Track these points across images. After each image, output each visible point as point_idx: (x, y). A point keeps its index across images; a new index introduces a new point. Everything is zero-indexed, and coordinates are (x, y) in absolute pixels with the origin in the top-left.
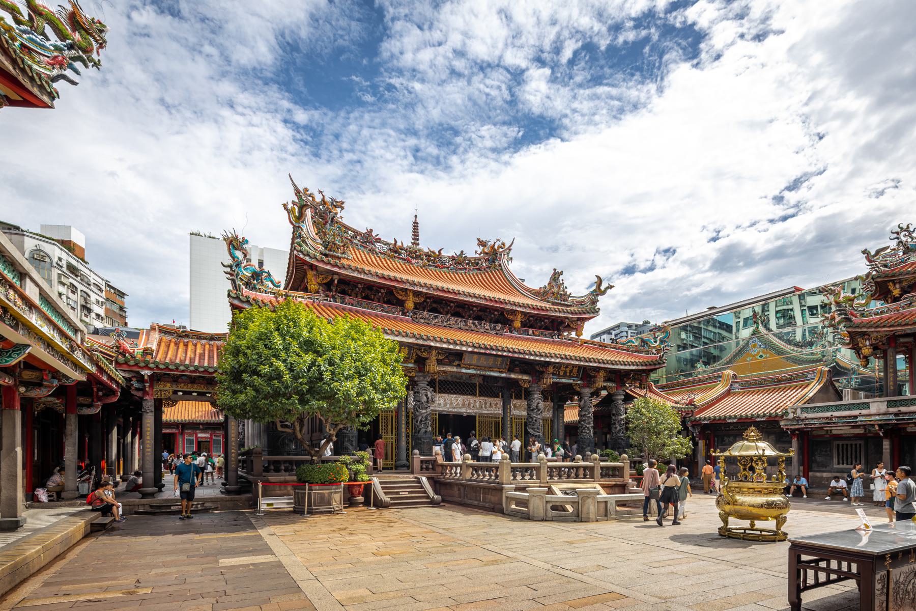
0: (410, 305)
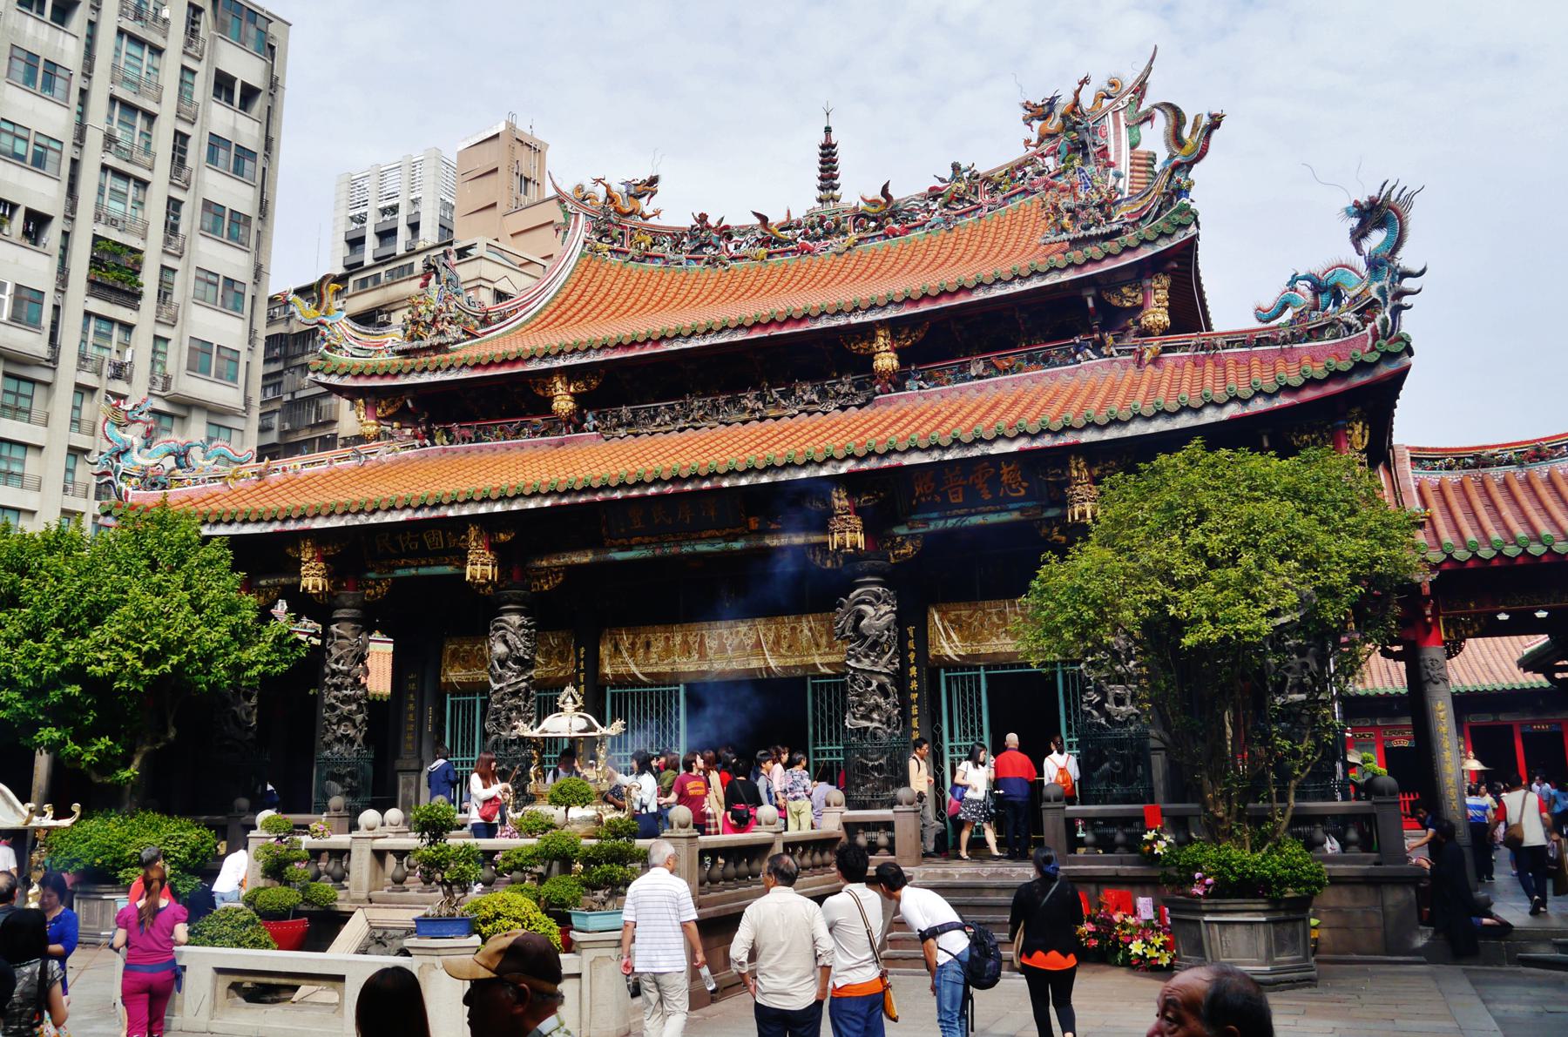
0: (563, 403)
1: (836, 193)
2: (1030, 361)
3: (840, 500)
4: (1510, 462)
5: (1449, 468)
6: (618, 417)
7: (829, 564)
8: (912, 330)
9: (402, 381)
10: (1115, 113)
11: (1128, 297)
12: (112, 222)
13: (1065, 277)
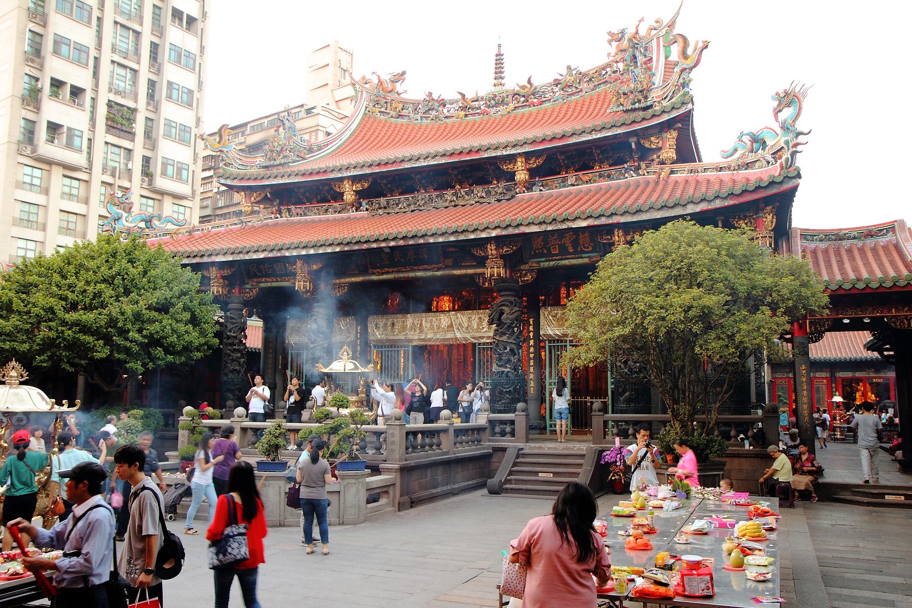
0: (349, 197)
1: (503, 81)
2: (600, 176)
3: (491, 249)
4: (854, 238)
5: (821, 240)
6: (379, 204)
8: (537, 158)
9: (267, 183)
11: (653, 142)
12: (118, 93)
13: (620, 131)
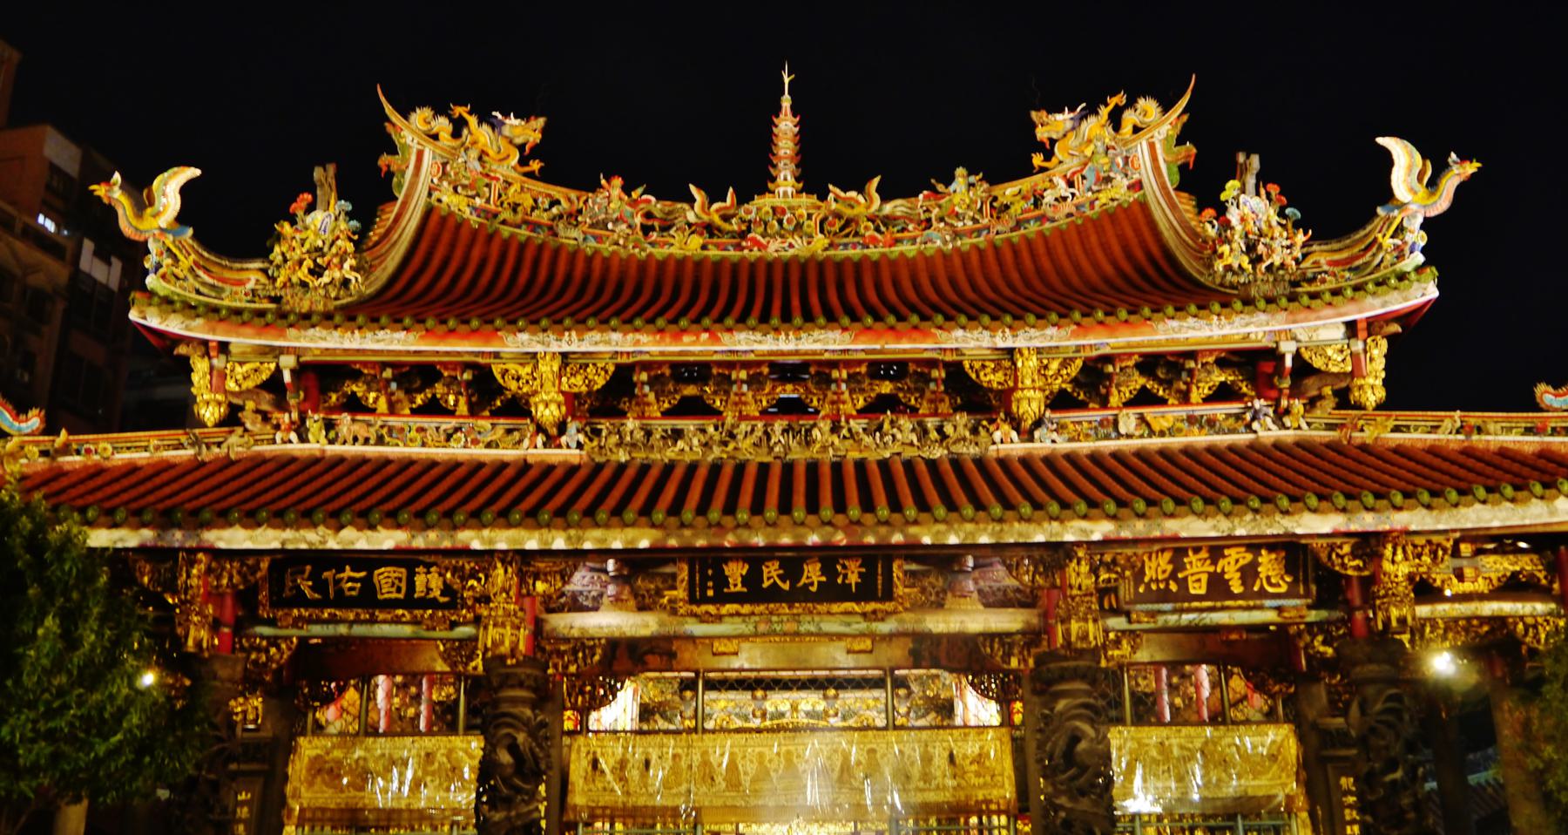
2: (1191, 420)
7: (1014, 663)
10: (1152, 146)
